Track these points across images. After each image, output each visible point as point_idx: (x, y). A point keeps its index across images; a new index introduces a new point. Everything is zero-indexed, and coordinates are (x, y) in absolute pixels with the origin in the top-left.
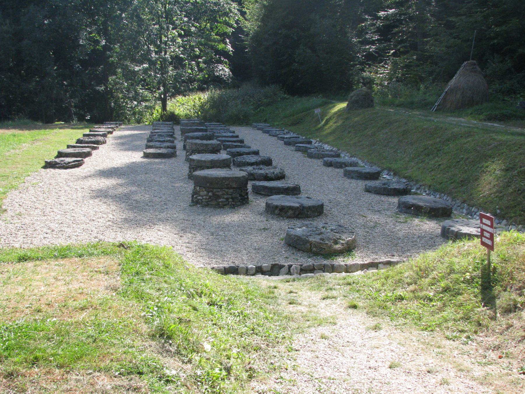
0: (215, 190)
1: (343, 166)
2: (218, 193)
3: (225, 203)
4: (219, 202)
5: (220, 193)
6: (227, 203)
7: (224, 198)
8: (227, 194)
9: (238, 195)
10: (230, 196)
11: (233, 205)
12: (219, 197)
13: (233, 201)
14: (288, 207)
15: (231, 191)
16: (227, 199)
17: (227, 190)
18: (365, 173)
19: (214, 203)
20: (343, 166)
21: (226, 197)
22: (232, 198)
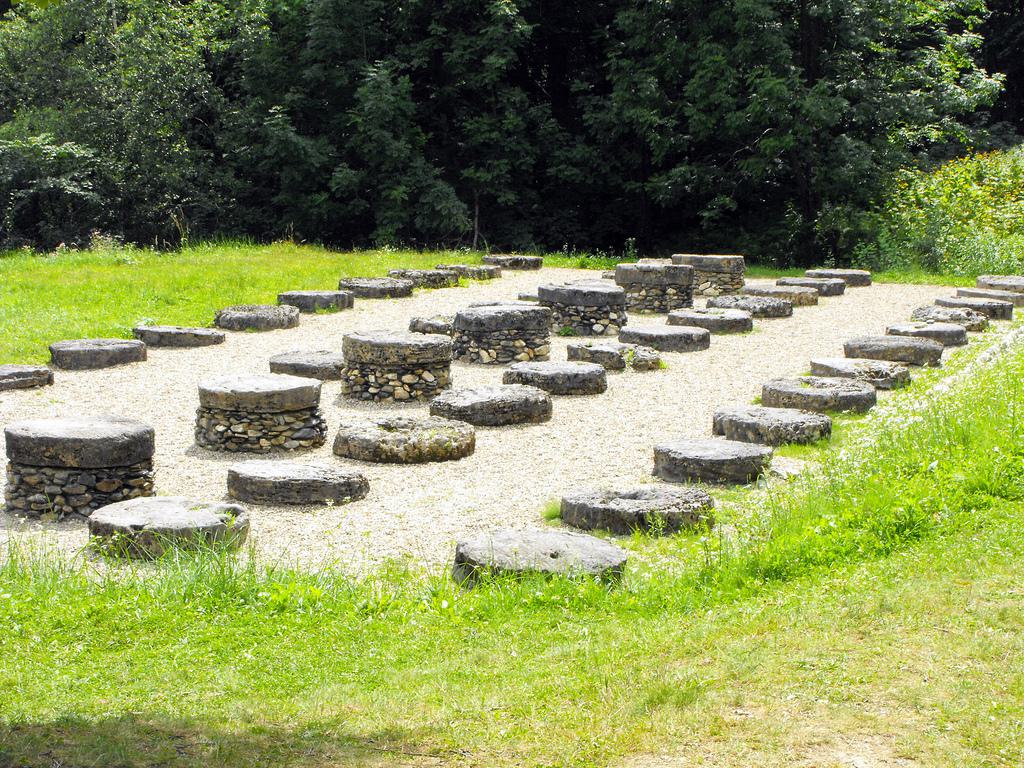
0: (23, 471)
1: (751, 435)
2: (27, 479)
3: (44, 507)
4: (30, 503)
5: (33, 480)
6: (50, 505)
7: (42, 493)
8: (53, 483)
9: (84, 488)
10: (57, 489)
11: (66, 514)
12: (32, 489)
13: (67, 502)
14: (103, 526)
15: (62, 474)
16: (52, 496)
17: (49, 472)
18: (685, 459)
19: (20, 503)
20: (751, 435)
21: (47, 489)
22: (64, 495)
